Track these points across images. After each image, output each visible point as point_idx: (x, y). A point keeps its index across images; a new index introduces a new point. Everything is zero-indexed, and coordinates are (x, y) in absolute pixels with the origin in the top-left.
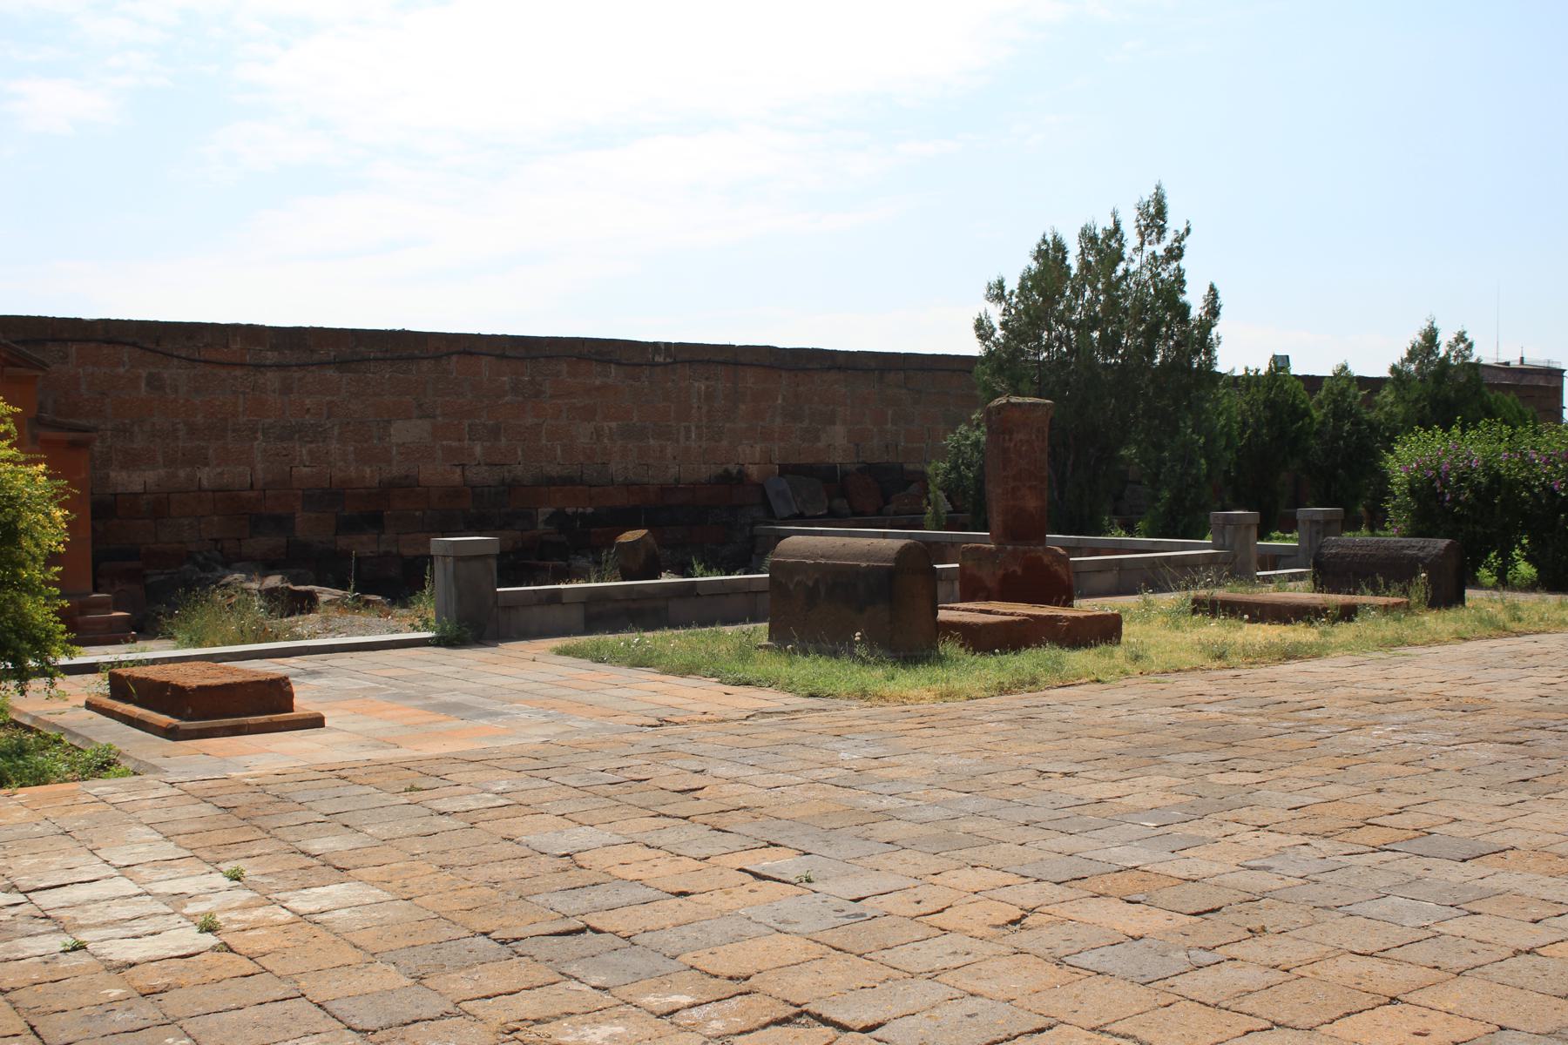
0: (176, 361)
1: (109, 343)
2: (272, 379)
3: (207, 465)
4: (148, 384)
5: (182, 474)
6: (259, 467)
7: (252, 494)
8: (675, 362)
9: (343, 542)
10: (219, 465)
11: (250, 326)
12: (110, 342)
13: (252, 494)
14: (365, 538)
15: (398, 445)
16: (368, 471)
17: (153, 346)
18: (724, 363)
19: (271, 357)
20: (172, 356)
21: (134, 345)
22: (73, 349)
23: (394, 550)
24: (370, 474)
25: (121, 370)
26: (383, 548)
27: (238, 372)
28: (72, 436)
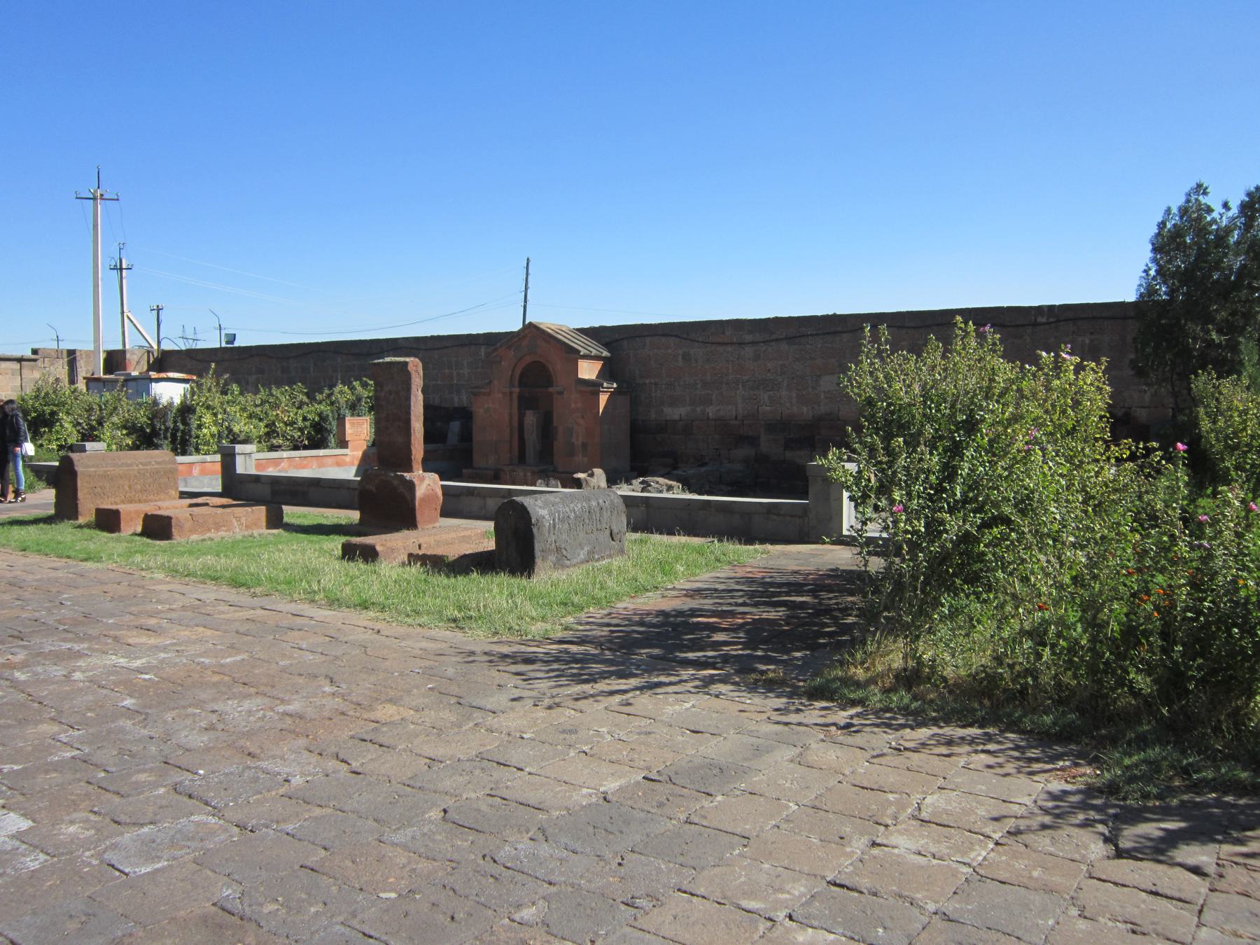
2: (748, 351)
8: (1058, 321)
12: (663, 335)
18: (1074, 320)
22: (648, 340)
24: (806, 412)
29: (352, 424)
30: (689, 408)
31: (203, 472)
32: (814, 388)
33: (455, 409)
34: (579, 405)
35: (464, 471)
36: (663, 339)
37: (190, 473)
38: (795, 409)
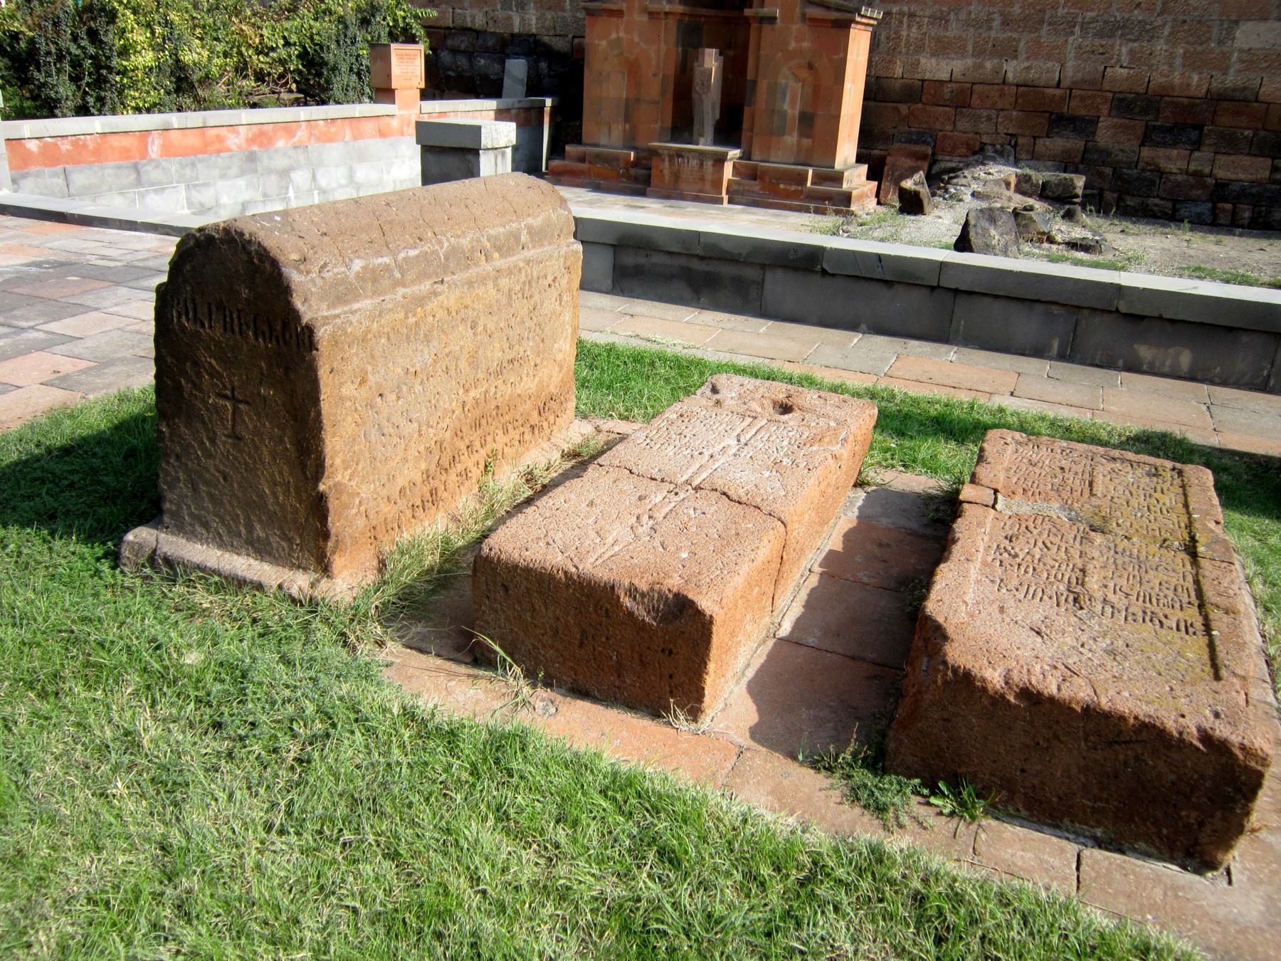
3: (1016, 57)
5: (988, 65)
6: (1070, 64)
7: (1058, 92)
9: (1146, 153)
10: (1028, 59)
14: (1175, 152)
15: (1241, 51)
23: (1207, 170)
24: (1197, 82)
26: (1192, 167)
28: (835, 15)
29: (401, 57)
30: (969, 62)
31: (168, 151)
32: (1220, 42)
33: (512, 35)
34: (806, 45)
35: (568, 148)
37: (144, 153)
38: (1177, 78)
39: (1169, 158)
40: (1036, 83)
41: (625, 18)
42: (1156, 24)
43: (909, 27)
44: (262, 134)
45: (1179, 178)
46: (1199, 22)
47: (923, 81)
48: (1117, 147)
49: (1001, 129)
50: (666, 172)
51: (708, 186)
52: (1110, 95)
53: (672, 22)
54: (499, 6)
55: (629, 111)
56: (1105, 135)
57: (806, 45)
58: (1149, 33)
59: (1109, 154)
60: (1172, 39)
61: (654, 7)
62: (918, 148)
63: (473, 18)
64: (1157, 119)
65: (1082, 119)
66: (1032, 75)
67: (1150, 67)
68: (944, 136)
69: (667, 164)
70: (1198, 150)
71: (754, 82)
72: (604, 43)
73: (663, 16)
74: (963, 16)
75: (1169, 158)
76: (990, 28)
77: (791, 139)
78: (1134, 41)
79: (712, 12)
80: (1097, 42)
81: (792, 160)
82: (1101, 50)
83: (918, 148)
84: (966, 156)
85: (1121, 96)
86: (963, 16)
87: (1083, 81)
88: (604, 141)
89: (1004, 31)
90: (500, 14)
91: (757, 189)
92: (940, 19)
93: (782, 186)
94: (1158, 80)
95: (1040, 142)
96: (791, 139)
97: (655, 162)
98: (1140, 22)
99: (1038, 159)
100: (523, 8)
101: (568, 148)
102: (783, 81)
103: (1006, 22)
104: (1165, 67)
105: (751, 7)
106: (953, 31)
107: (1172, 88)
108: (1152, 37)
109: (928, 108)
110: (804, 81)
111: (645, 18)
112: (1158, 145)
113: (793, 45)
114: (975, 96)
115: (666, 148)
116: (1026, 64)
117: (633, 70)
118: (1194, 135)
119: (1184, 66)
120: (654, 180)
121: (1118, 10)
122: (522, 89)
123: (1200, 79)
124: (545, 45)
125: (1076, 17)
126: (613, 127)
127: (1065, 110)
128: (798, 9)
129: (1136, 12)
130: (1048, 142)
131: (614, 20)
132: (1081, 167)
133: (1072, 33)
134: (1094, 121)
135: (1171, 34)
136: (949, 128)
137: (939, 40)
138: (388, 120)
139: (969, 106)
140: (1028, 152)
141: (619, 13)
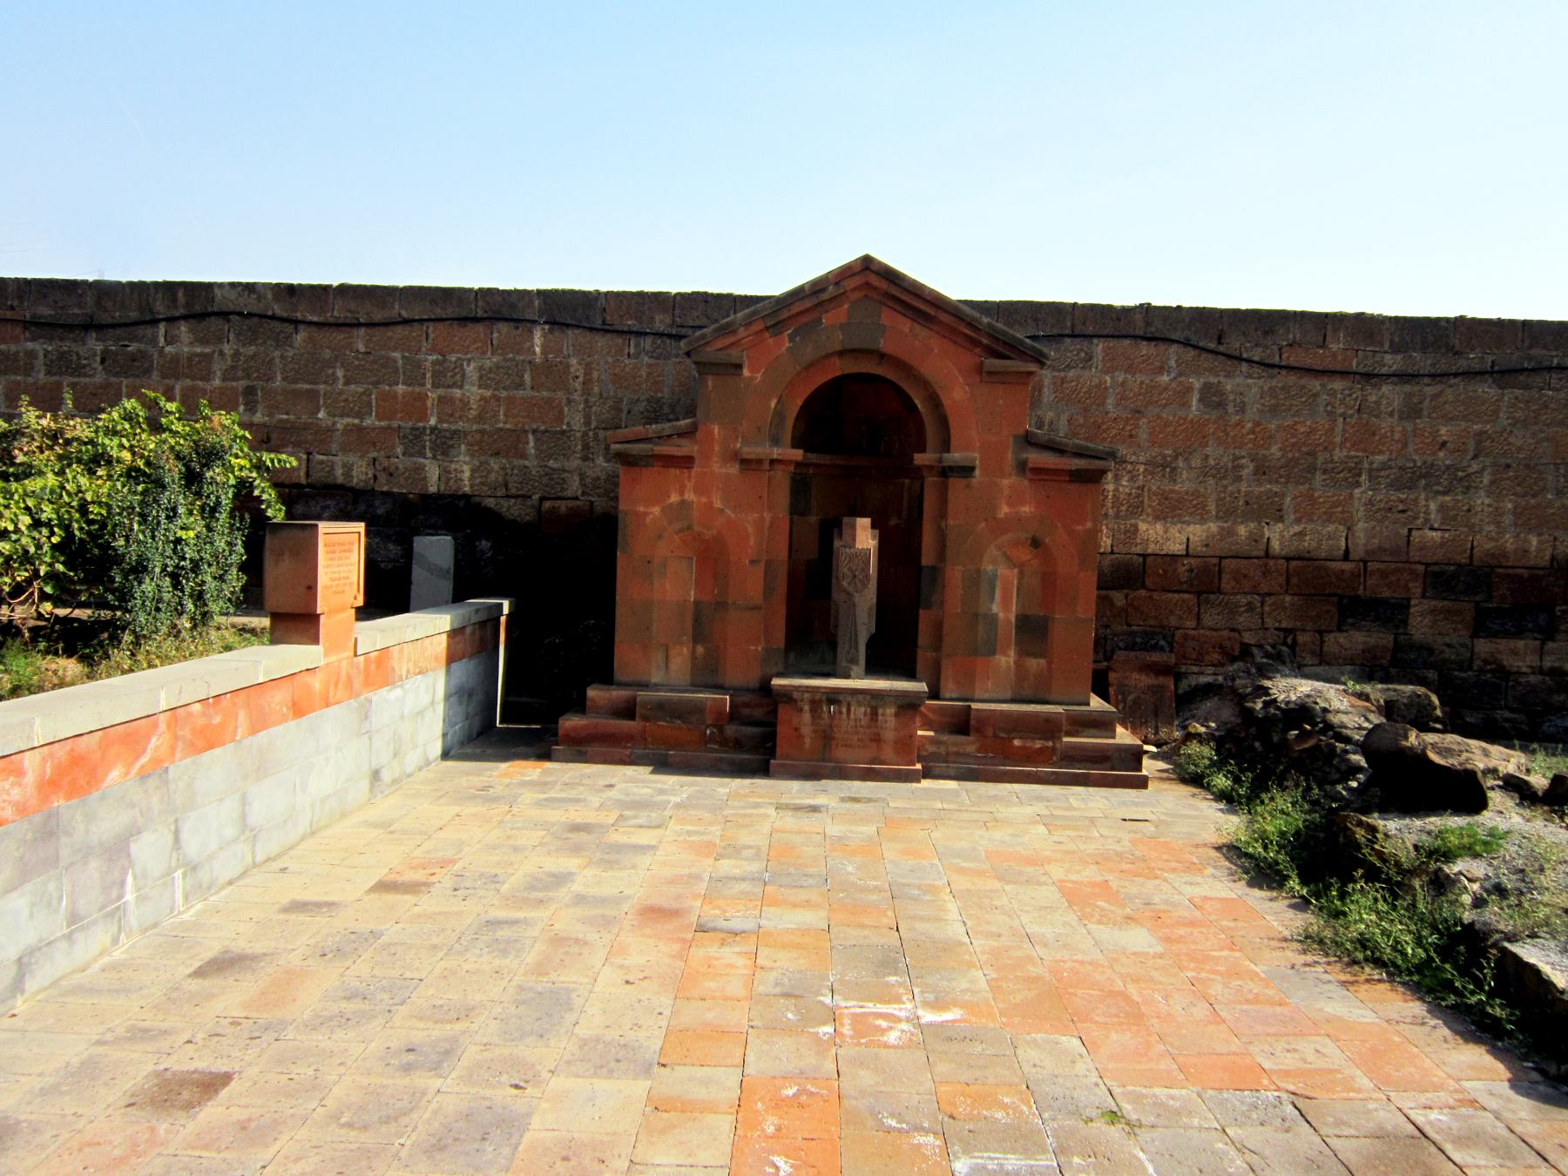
0: (1244, 367)
1: (1149, 339)
2: (1390, 395)
3: (1281, 519)
4: (1200, 400)
6: (1361, 526)
7: (1347, 566)
9: (1483, 647)
10: (1298, 521)
11: (1360, 318)
13: (1347, 566)
14: (1521, 644)
16: (1534, 541)
17: (1212, 346)
19: (1392, 362)
20: (1240, 359)
21: (1187, 344)
22: (1099, 347)
25: (1165, 378)
26: (1548, 663)
27: (1338, 384)
30: (1213, 527)
33: (426, 497)
34: (1026, 509)
35: (593, 693)
36: (1145, 348)
38: (1509, 541)
39: (1514, 653)
40: (1314, 554)
41: (696, 470)
42: (1471, 470)
43: (1117, 478)
44: (76, 761)
45: (1533, 679)
46: (1527, 466)
47: (1145, 556)
48: (1439, 639)
49: (1269, 622)
50: (807, 730)
51: (888, 752)
52: (1421, 568)
53: (782, 478)
54: (399, 450)
55: (703, 624)
56: (1422, 623)
57: (1026, 509)
58: (1467, 484)
59: (1431, 651)
60: (1495, 489)
61: (751, 451)
62: (1155, 657)
63: (348, 469)
64: (1490, 598)
65: (1384, 602)
66: (1308, 543)
67: (1471, 528)
68: (1185, 637)
69: (807, 716)
70: (1552, 639)
71: (936, 572)
72: (656, 510)
73: (766, 466)
74: (1196, 462)
75: (1514, 653)
76: (1239, 479)
77: (1006, 660)
78: (1445, 493)
79: (826, 459)
80: (1395, 495)
81: (1009, 695)
82: (1401, 507)
83: (1155, 657)
84: (1222, 665)
85: (1436, 568)
86: (1196, 462)
87: (1381, 549)
88: (657, 677)
89: (1260, 485)
90: (401, 462)
91: (971, 748)
92: (1164, 467)
93: (1016, 742)
94: (1483, 545)
95: (1330, 638)
96: (1006, 660)
97: (783, 712)
98: (1448, 467)
99: (1328, 664)
100: (445, 453)
101: (593, 693)
102: (990, 568)
103: (1261, 470)
104: (1492, 527)
105: (923, 450)
106: (1185, 483)
107: (1504, 554)
108: (1468, 488)
109: (1155, 595)
110: (1021, 567)
111: (734, 469)
112: (1494, 635)
113: (1004, 510)
114: (1225, 578)
115: (808, 689)
116: (1297, 528)
117: (710, 556)
118: (1542, 619)
119: (1516, 525)
120: (782, 746)
121: (1416, 451)
122: (447, 586)
123: (1540, 543)
124: (488, 511)
125: (1361, 462)
126: (673, 652)
127: (1361, 591)
128: (1010, 456)
129: (1441, 454)
130: (1342, 638)
131: (674, 472)
132: (1393, 671)
133: (1358, 484)
134: (1404, 606)
135: (1492, 483)
136: (1191, 623)
137: (1164, 496)
138: (308, 678)
139: (1219, 591)
140: (1313, 653)
141: (686, 462)
